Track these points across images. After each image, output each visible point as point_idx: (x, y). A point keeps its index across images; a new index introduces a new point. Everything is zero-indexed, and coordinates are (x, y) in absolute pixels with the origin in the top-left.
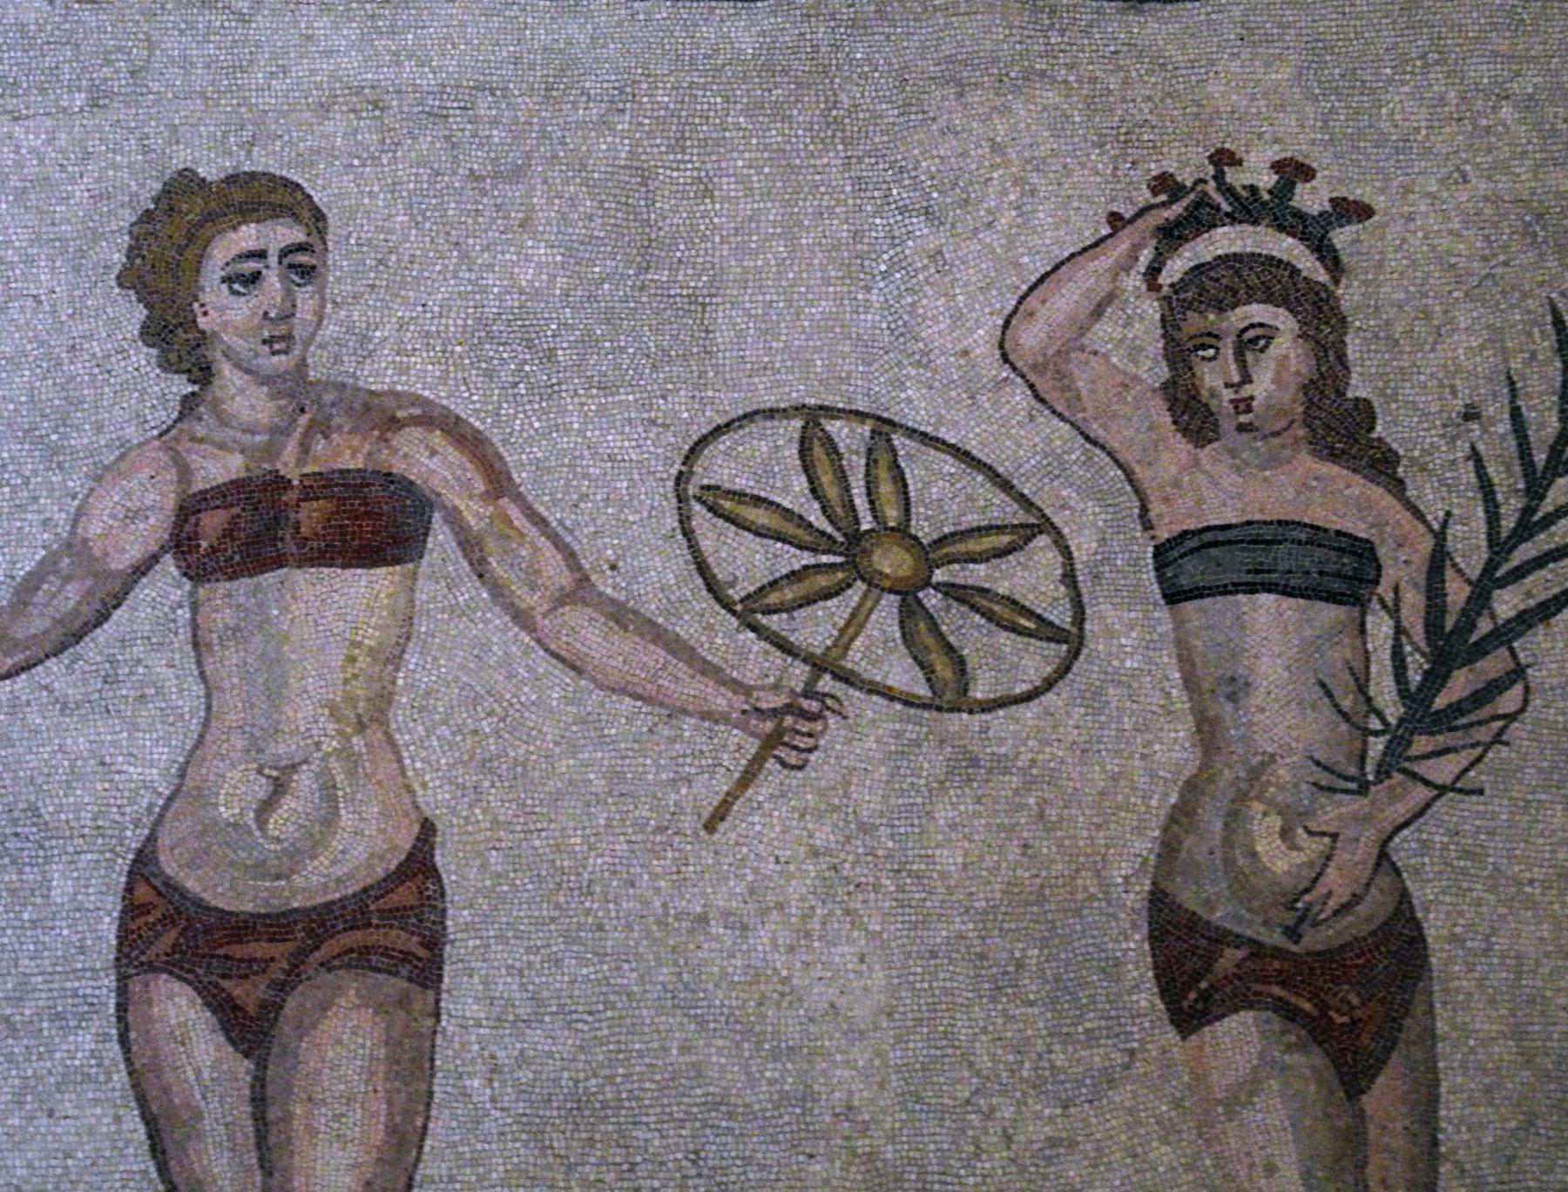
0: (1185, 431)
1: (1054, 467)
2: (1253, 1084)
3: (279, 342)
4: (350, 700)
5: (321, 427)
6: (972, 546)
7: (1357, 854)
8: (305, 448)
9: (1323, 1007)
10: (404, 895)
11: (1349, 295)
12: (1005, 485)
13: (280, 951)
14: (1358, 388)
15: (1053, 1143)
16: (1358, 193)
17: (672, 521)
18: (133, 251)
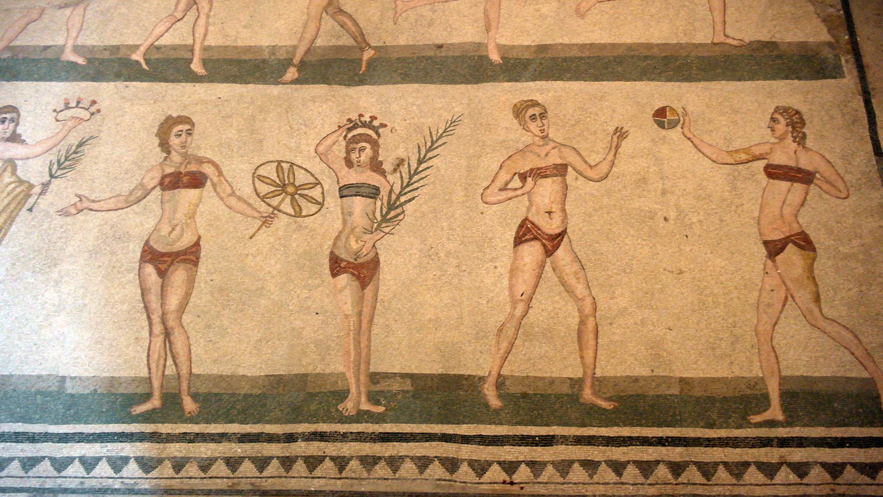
0: (347, 166)
1: (322, 172)
2: (345, 288)
3: (183, 147)
4: (188, 213)
5: (189, 163)
6: (305, 187)
7: (371, 244)
8: (186, 166)
9: (359, 273)
10: (194, 249)
11: (381, 141)
12: (313, 176)
13: (169, 259)
14: (380, 159)
15: (306, 298)
16: (385, 122)
17: (251, 182)
18: (159, 130)
